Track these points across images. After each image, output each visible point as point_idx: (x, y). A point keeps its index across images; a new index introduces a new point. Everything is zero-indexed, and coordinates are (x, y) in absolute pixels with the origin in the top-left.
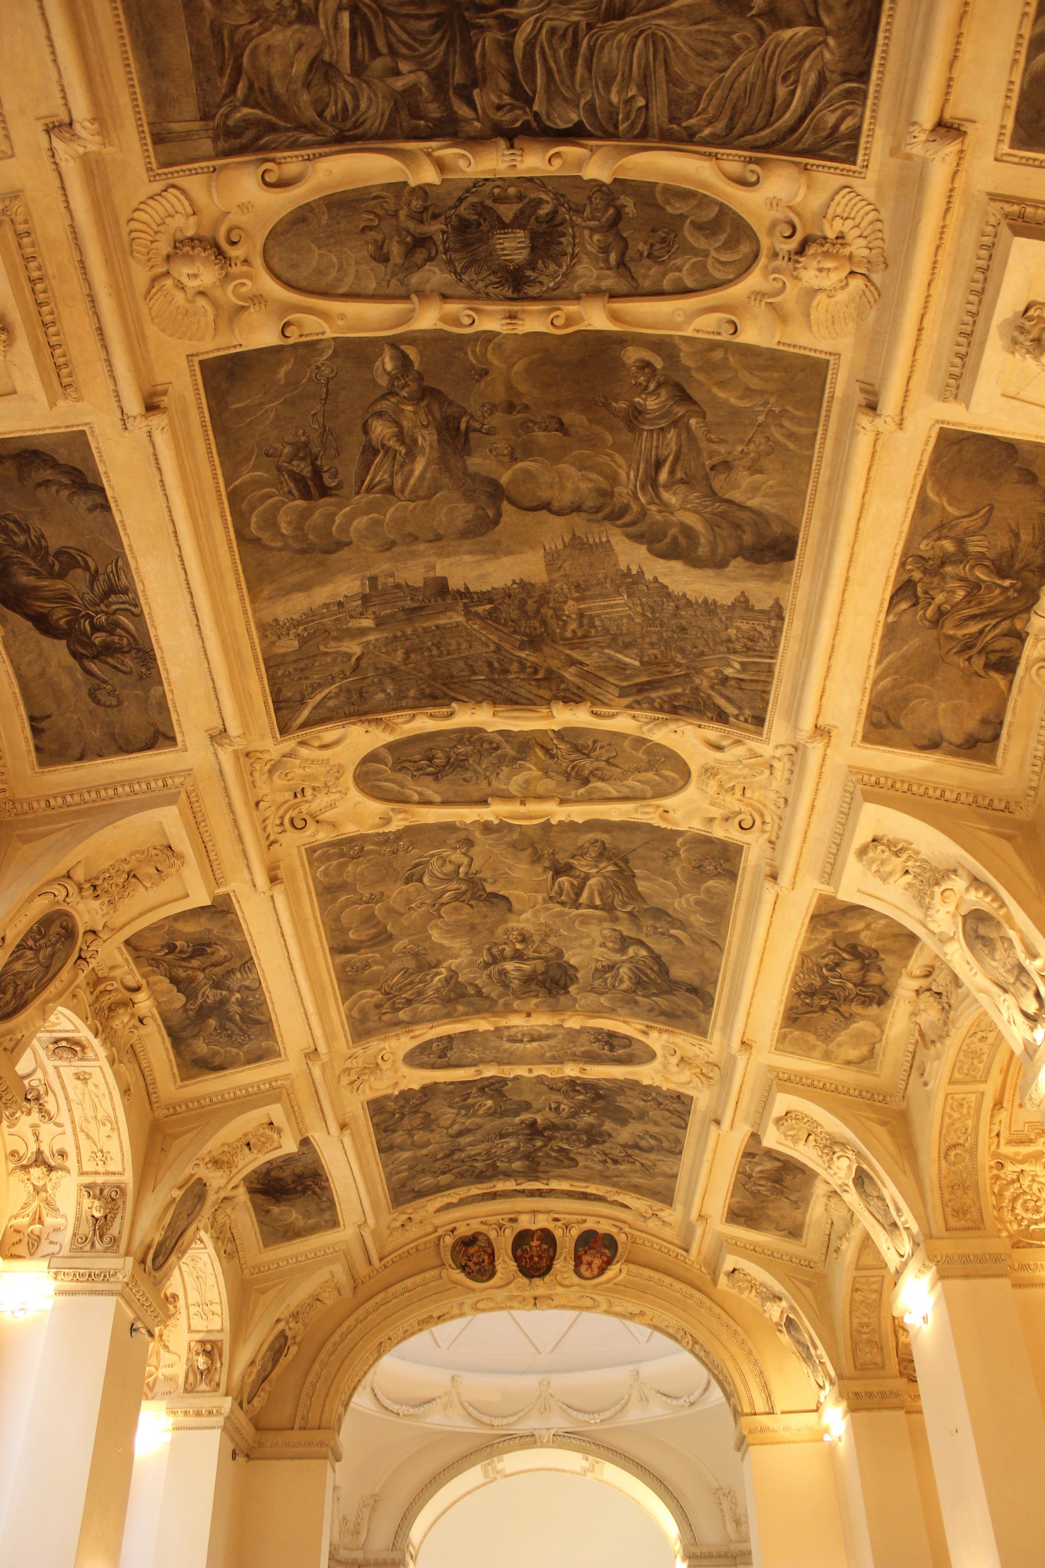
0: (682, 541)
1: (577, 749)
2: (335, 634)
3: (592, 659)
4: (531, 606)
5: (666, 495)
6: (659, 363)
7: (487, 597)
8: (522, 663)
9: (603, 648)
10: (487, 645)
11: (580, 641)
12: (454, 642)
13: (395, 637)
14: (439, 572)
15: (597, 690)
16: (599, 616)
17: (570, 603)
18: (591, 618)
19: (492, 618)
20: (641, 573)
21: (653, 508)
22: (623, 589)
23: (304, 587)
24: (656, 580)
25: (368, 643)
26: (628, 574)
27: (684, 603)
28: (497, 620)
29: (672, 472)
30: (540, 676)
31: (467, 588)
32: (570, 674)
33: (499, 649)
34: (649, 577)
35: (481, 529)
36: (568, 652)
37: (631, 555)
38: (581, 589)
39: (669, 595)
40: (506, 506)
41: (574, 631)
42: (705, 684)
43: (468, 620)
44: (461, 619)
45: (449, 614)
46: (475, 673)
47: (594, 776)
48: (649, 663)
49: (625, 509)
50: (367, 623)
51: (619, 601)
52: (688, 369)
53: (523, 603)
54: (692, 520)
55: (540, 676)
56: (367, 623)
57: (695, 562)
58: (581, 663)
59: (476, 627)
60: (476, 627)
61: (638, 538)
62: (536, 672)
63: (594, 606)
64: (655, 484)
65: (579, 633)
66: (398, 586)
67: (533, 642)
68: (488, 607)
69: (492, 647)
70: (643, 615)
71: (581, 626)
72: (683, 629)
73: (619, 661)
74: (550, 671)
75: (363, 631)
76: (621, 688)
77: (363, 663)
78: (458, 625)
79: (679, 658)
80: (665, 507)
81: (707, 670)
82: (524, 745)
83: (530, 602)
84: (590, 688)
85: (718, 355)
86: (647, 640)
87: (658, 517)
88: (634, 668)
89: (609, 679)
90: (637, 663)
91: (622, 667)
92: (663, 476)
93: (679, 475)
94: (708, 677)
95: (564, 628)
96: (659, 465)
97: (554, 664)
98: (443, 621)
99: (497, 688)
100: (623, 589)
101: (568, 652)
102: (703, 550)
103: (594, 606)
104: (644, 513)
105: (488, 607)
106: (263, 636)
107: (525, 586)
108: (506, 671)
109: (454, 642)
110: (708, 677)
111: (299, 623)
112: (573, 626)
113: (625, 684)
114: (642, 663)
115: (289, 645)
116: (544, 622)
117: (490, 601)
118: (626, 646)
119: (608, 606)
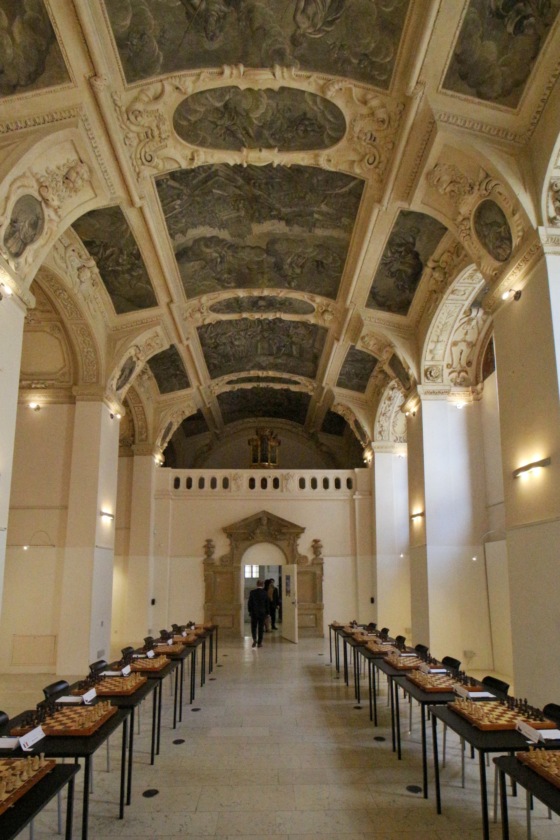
0: (209, 243)
1: (233, 134)
2: (328, 216)
3: (232, 190)
4: (257, 214)
5: (217, 255)
6: (226, 284)
7: (273, 217)
8: (260, 189)
9: (228, 196)
10: (274, 197)
11: (238, 198)
12: (286, 200)
13: (307, 206)
14: (288, 228)
15: (228, 172)
16: (232, 210)
17: (243, 215)
18: (234, 209)
19: (271, 209)
20: (220, 230)
21: (220, 251)
22: (225, 222)
23: (332, 237)
24: (214, 228)
25: (318, 207)
26: (223, 228)
27: (203, 224)
28: (270, 208)
29: (217, 261)
30: (253, 181)
31: (279, 221)
32: (240, 181)
33: (269, 195)
34: (217, 228)
35: (273, 241)
36: (242, 193)
37: (224, 234)
38: (239, 220)
39: (209, 224)
40: (265, 247)
41: (240, 203)
42: (185, 191)
43: (280, 209)
44: (282, 209)
45: (287, 212)
46: (279, 183)
47: (222, 112)
48: (209, 192)
49: (228, 248)
50: (316, 216)
51: (225, 218)
52: (219, 285)
53: (260, 215)
54: (208, 250)
55: (253, 181)
56: (316, 216)
57: (204, 238)
58: (236, 187)
59: (277, 205)
60: (277, 205)
61: (223, 240)
62: (254, 183)
63: (234, 214)
64: (221, 257)
65: (238, 202)
66: (303, 226)
67: (255, 199)
68: (272, 213)
69: (272, 196)
70: (216, 214)
71: (238, 206)
72: (200, 213)
73: (220, 190)
74: (249, 184)
75: (319, 213)
76: (218, 175)
77: (322, 199)
78: (284, 207)
79: (198, 199)
80: (216, 252)
81: (187, 198)
82: (259, 141)
83: (257, 216)
84: (231, 174)
85: (212, 289)
86: (212, 203)
87: (218, 248)
88: (214, 188)
89: (223, 180)
90: (214, 191)
91: (220, 187)
92: (219, 260)
93: (215, 262)
94: (185, 195)
95: (244, 205)
96: (221, 262)
97: (247, 187)
98: (289, 210)
99: (271, 174)
100: (225, 222)
101: (242, 193)
102: (202, 243)
103: (234, 214)
104: (223, 248)
105: (272, 213)
106: (351, 229)
107: (259, 222)
108: (266, 184)
109: (286, 200)
110: (185, 195)
111: (339, 227)
112: (241, 205)
113: (217, 178)
114: (212, 192)
115: (345, 221)
116: (252, 208)
117: (271, 216)
118: (219, 198)
119: (228, 215)
